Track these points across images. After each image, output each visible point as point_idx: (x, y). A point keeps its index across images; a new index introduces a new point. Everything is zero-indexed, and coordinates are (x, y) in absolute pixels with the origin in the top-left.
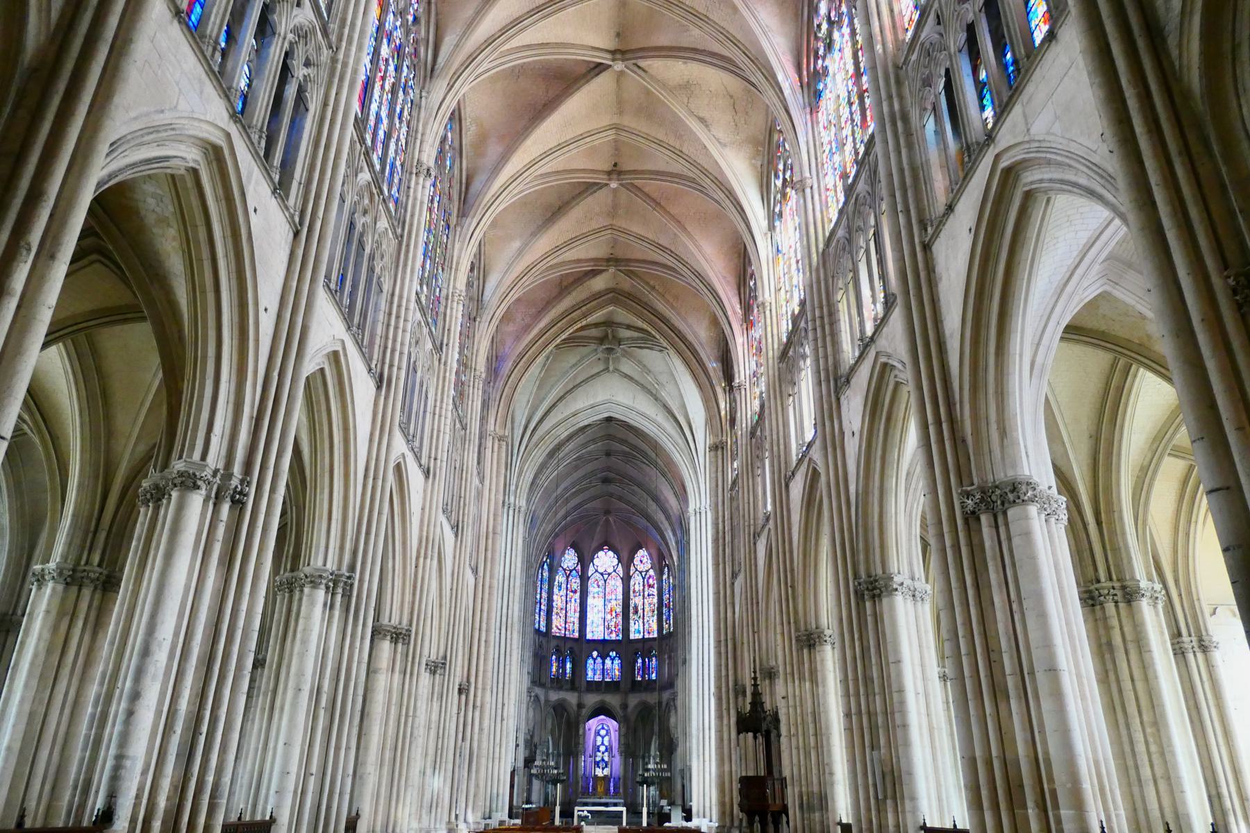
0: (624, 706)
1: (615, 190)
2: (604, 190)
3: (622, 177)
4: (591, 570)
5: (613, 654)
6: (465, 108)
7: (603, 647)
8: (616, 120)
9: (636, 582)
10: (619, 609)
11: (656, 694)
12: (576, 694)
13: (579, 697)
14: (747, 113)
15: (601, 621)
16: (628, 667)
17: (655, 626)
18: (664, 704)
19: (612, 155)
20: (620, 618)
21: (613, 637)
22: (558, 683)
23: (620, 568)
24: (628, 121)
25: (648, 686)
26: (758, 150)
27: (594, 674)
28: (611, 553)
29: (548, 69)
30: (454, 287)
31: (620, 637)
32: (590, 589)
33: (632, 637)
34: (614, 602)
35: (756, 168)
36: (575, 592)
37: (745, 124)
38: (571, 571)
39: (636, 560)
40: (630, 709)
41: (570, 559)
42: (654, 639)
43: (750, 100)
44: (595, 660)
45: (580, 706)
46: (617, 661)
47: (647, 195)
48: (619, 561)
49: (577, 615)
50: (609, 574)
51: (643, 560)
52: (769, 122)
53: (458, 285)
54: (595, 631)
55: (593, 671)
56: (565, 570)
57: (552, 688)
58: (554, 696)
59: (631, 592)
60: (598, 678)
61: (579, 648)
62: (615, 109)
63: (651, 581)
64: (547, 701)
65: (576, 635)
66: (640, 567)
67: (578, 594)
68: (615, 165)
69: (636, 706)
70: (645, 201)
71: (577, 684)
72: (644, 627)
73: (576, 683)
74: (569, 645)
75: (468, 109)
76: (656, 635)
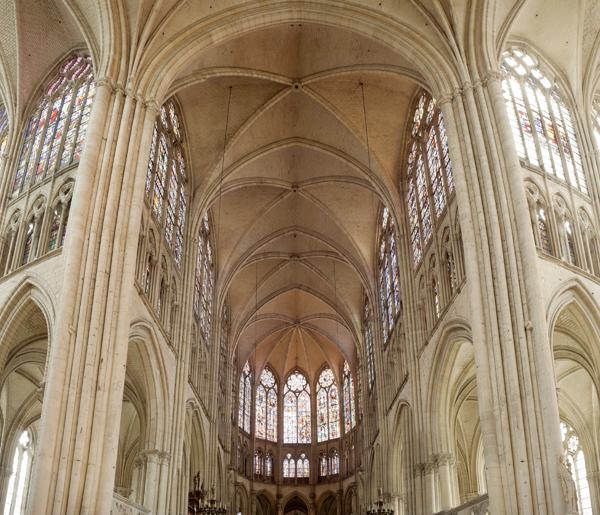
0: (313, 496)
4: (286, 389)
5: (303, 455)
7: (296, 450)
9: (322, 395)
10: (309, 420)
11: (338, 484)
12: (274, 487)
13: (278, 490)
15: (295, 430)
16: (315, 467)
17: (338, 429)
18: (345, 490)
20: (309, 426)
21: (305, 441)
22: (261, 478)
23: (308, 388)
25: (331, 479)
27: (289, 473)
28: (300, 376)
31: (310, 442)
32: (285, 404)
33: (319, 440)
34: (304, 414)
36: (274, 405)
38: (270, 389)
39: (321, 380)
40: (317, 498)
41: (267, 378)
42: (336, 440)
44: (289, 461)
45: (279, 496)
46: (307, 462)
48: (308, 382)
49: (276, 424)
50: (300, 392)
51: (328, 377)
54: (290, 437)
55: (289, 469)
56: (264, 387)
57: (256, 481)
58: (258, 487)
59: (318, 407)
60: (292, 475)
61: (277, 450)
63: (333, 394)
64: (252, 490)
65: (275, 440)
66: (324, 386)
67: (275, 408)
69: (322, 496)
71: (276, 479)
72: (331, 431)
73: (275, 478)
74: (269, 447)
76: (339, 436)
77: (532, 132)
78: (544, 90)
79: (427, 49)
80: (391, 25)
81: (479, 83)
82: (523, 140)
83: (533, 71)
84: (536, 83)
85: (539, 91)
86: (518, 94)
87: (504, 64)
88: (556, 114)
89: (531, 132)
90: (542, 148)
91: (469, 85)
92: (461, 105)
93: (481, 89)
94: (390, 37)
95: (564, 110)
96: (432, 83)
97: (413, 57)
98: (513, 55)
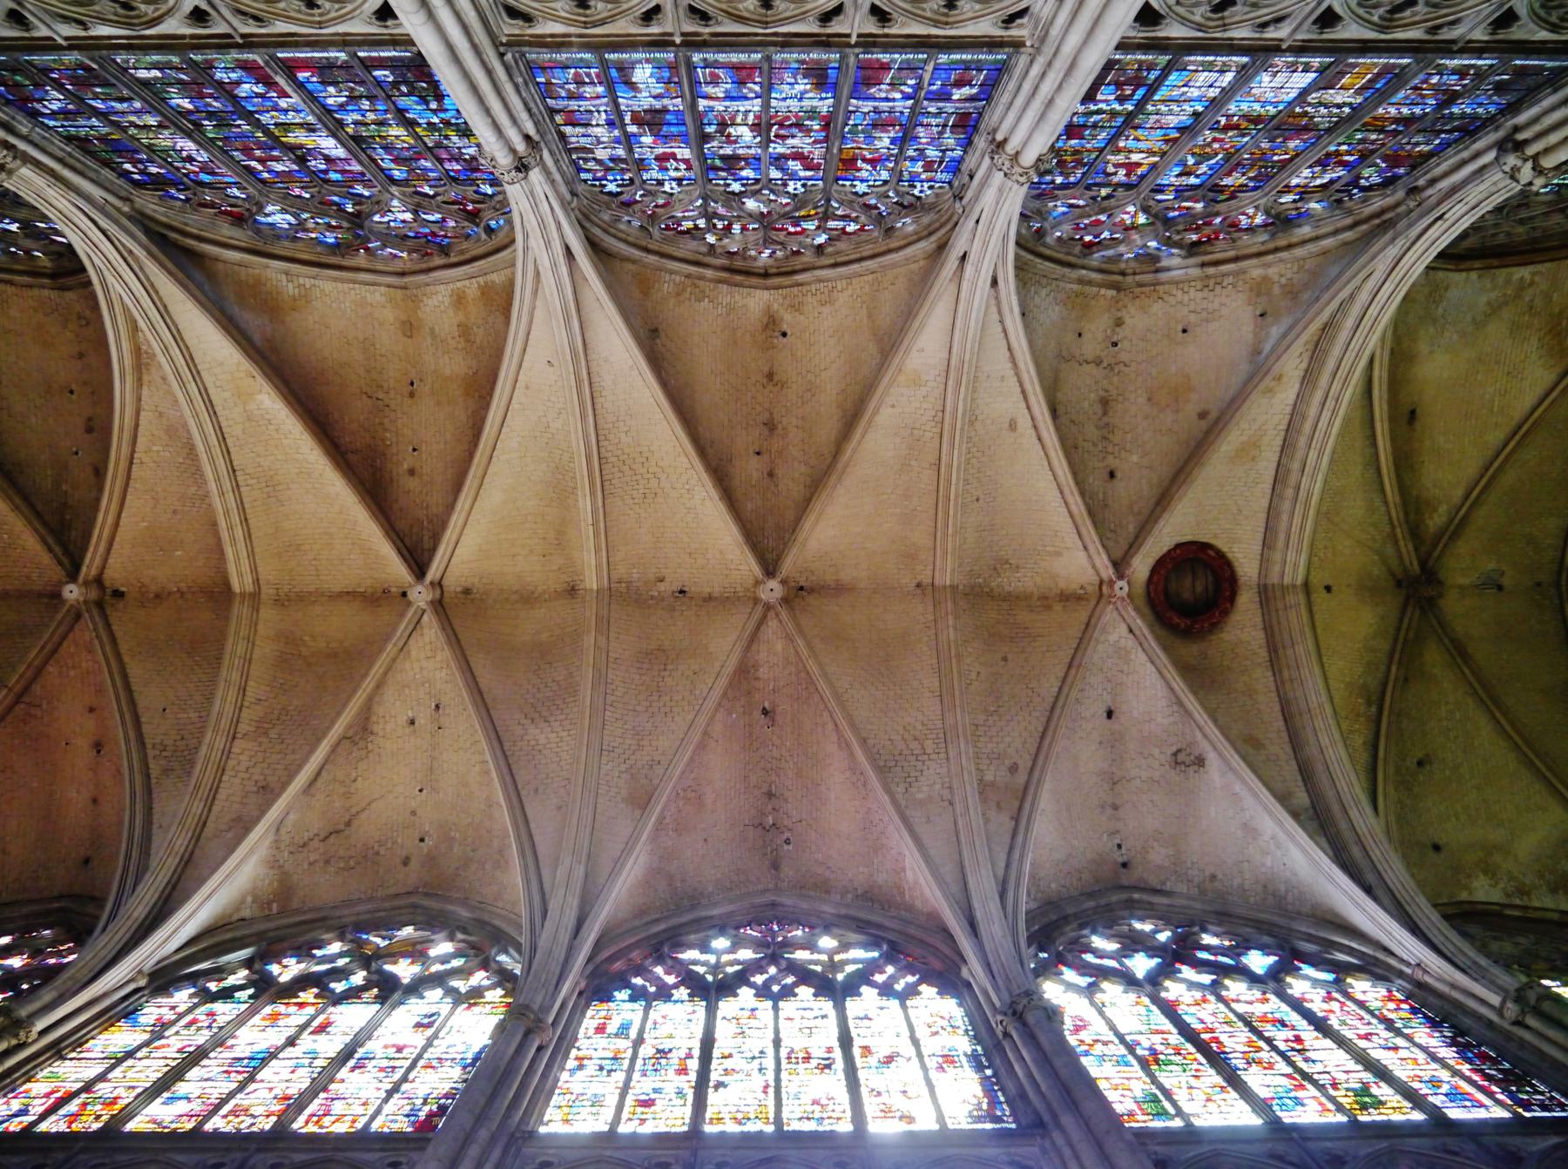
1: (56, 596)
2: (58, 573)
3: (95, 612)
6: (335, 280)
8: (267, 592)
14: (327, 862)
19: (144, 586)
24: (267, 613)
26: (269, 903)
29: (384, 455)
30: (27, 159)
35: (238, 909)
37: (310, 864)
43: (352, 863)
47: (39, 671)
52: (338, 913)
53: (25, 171)
62: (286, 588)
68: (117, 594)
70: (29, 666)
75: (328, 286)
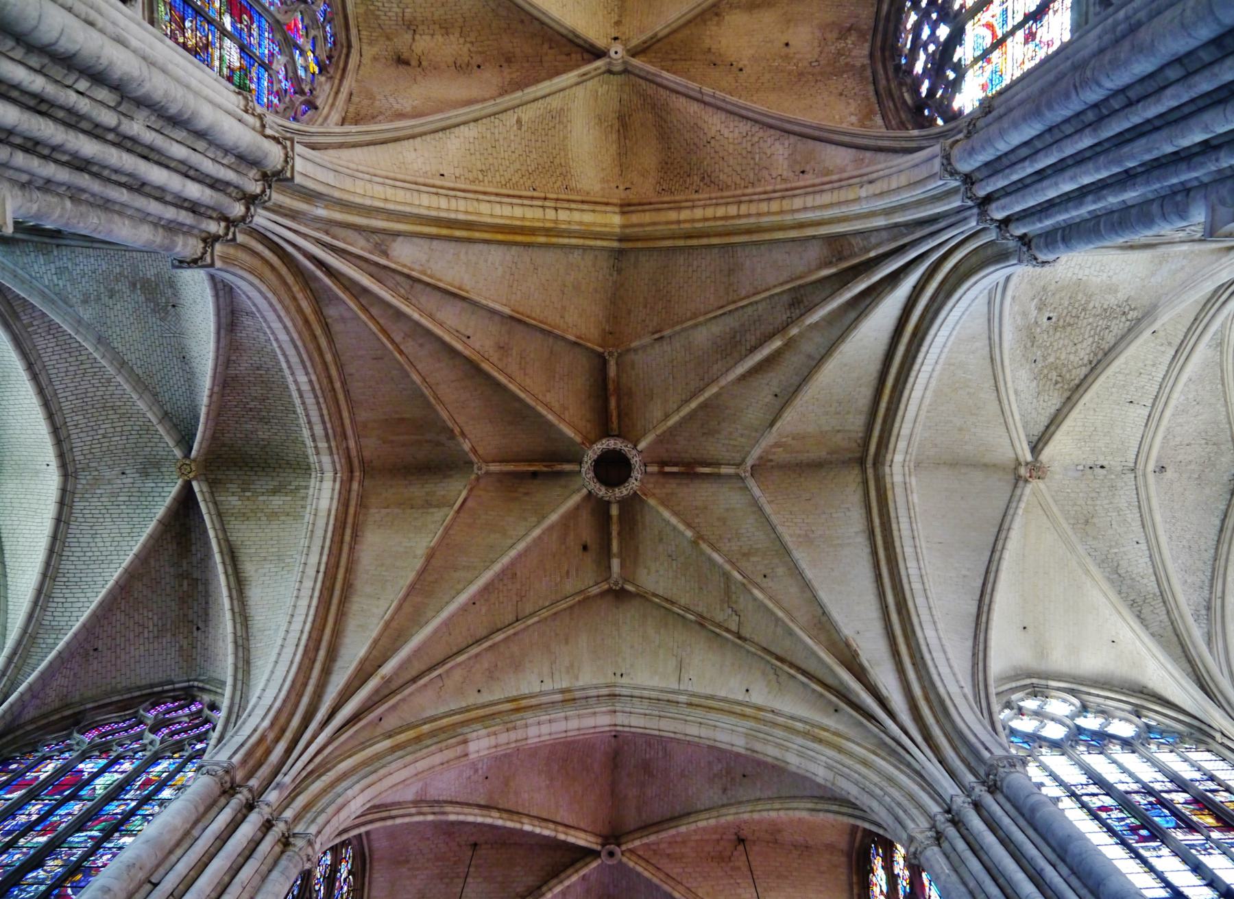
77: (1157, 834)
78: (1126, 743)
79: (851, 755)
80: (775, 724)
81: (980, 791)
82: (1144, 861)
83: (1081, 722)
84: (1101, 740)
85: (1115, 750)
86: (1074, 776)
87: (1013, 732)
88: (1188, 773)
89: (1152, 838)
90: (1205, 859)
91: (960, 801)
92: (961, 845)
93: (988, 799)
94: (777, 745)
95: (1202, 757)
96: (882, 815)
97: (830, 776)
98: (1021, 712)
